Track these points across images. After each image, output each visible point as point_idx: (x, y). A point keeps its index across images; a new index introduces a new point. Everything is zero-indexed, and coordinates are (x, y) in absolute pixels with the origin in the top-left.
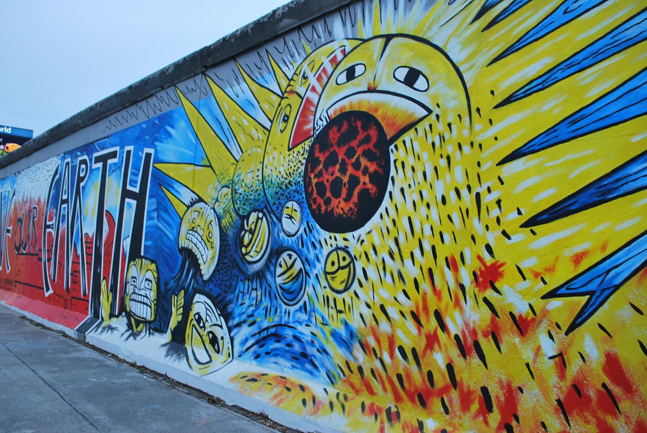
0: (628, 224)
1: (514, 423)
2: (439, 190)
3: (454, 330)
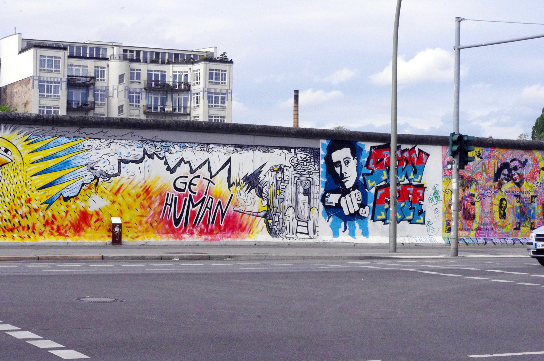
0: (56, 191)
1: (35, 231)
2: (15, 181)
3: (20, 213)
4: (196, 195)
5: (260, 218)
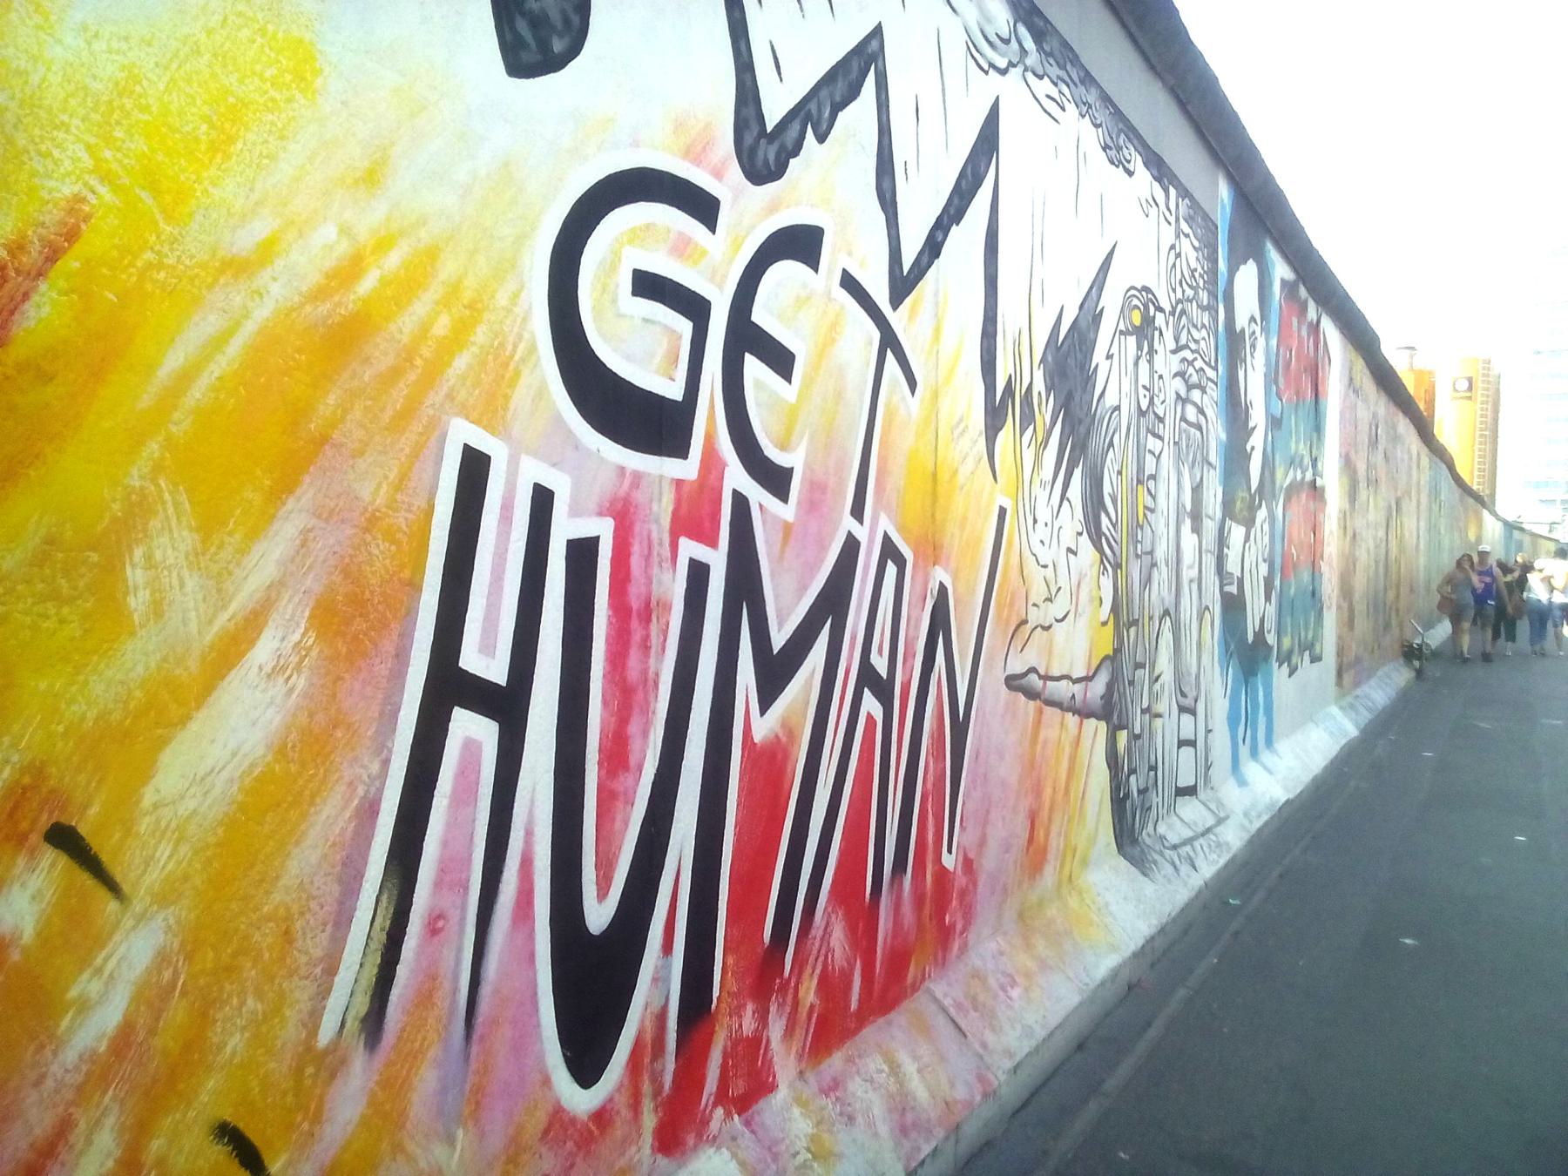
4: (787, 511)
5: (1093, 721)
